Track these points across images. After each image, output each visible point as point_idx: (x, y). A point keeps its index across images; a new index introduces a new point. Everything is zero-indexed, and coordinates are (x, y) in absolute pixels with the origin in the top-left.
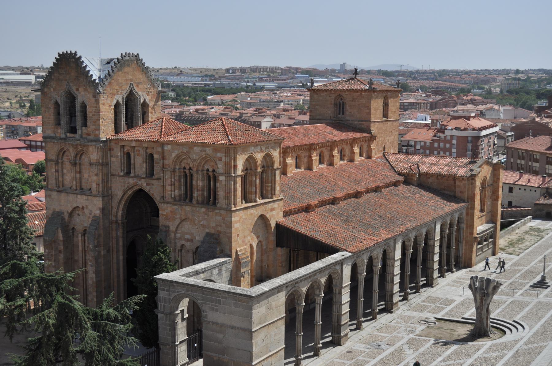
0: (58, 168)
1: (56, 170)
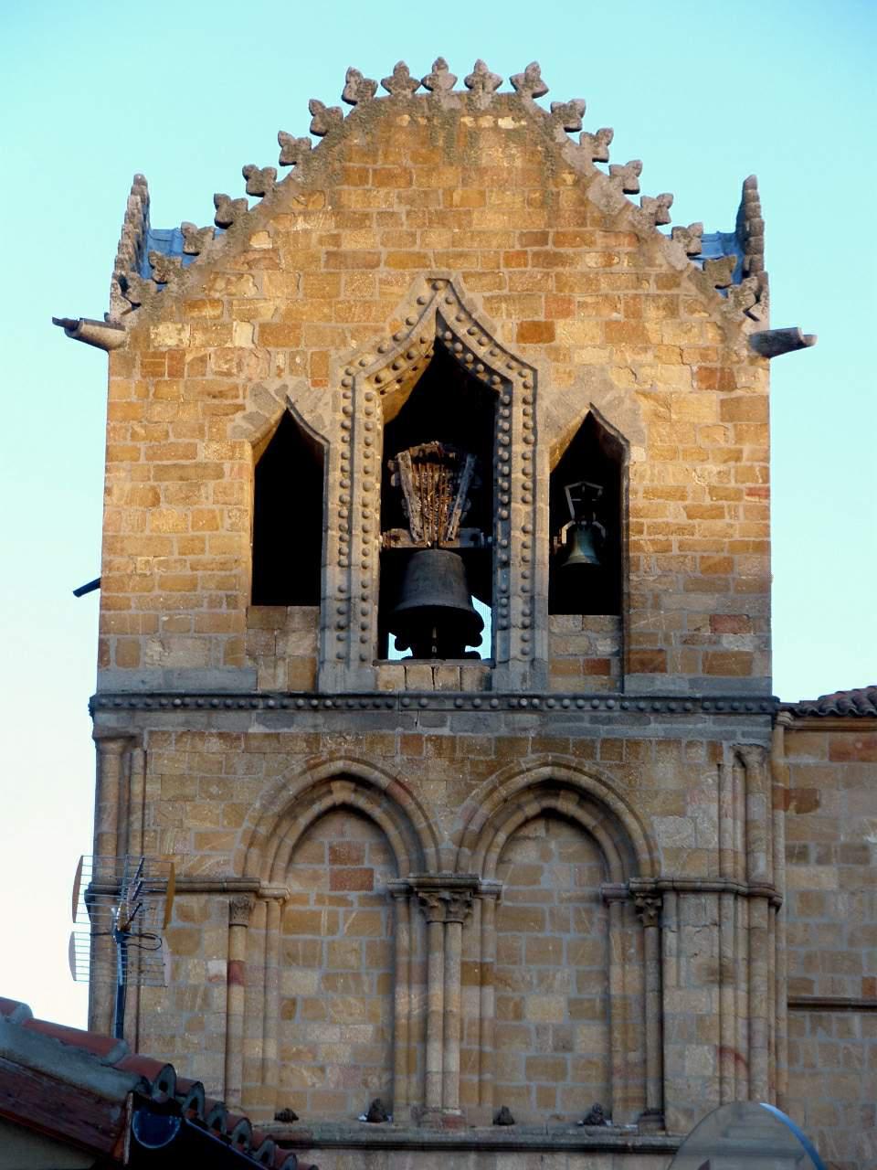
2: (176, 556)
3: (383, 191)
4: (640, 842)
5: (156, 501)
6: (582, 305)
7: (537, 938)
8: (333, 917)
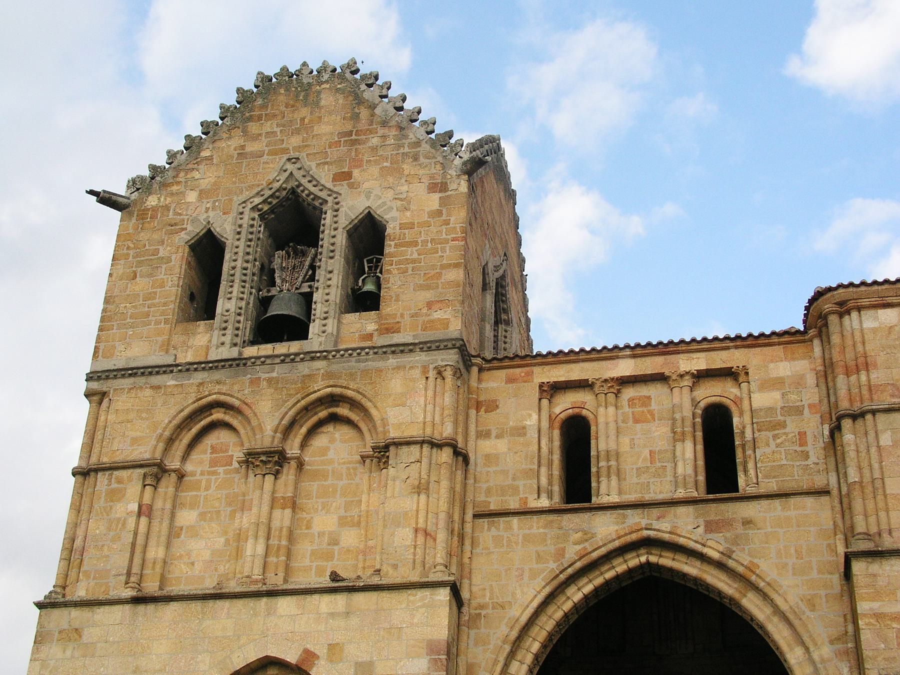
0: (153, 499)
1: (140, 507)
2: (141, 302)
3: (269, 123)
4: (378, 423)
5: (135, 277)
6: (369, 161)
7: (323, 485)
8: (209, 481)
